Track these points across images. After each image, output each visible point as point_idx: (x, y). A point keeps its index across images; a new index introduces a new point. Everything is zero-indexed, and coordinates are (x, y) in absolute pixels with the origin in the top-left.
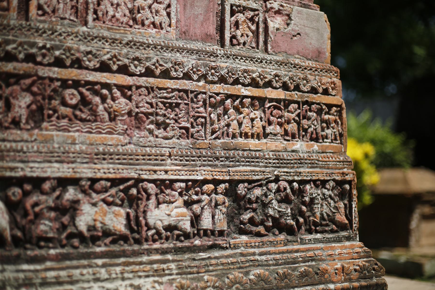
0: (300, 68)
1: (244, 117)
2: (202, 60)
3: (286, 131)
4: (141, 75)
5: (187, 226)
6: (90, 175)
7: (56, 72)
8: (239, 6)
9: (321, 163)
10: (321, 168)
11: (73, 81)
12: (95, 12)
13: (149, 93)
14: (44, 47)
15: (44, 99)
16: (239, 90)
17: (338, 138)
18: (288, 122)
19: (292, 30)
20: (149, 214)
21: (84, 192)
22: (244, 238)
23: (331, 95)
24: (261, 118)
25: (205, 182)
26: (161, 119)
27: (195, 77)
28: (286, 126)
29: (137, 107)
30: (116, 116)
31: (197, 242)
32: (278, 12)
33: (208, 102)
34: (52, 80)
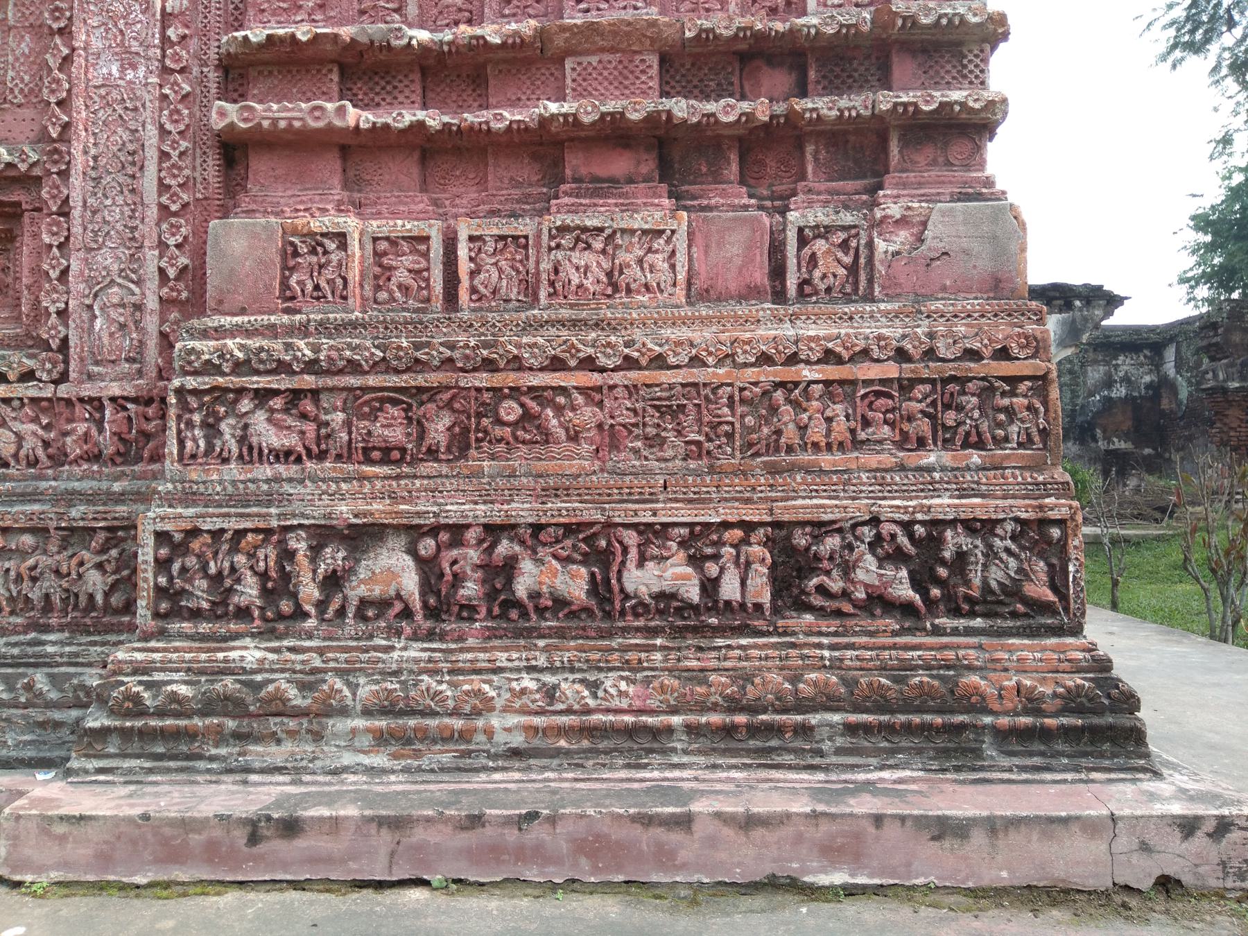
0: (942, 316)
1: (810, 418)
2: (728, 331)
3: (905, 436)
5: (693, 593)
6: (530, 520)
7: (482, 379)
8: (817, 226)
9: (984, 488)
10: (983, 496)
11: (511, 388)
12: (552, 284)
13: (630, 394)
14: (467, 346)
15: (469, 418)
16: (797, 372)
17: (1037, 439)
18: (910, 419)
19: (930, 249)
20: (625, 574)
21: (522, 543)
22: (809, 618)
23: (1018, 359)
24: (847, 417)
25: (726, 525)
26: (651, 431)
27: (710, 360)
28: (906, 426)
29: (612, 417)
30: (577, 433)
31: (713, 621)
32: (903, 222)
33: (737, 398)
34: (478, 390)
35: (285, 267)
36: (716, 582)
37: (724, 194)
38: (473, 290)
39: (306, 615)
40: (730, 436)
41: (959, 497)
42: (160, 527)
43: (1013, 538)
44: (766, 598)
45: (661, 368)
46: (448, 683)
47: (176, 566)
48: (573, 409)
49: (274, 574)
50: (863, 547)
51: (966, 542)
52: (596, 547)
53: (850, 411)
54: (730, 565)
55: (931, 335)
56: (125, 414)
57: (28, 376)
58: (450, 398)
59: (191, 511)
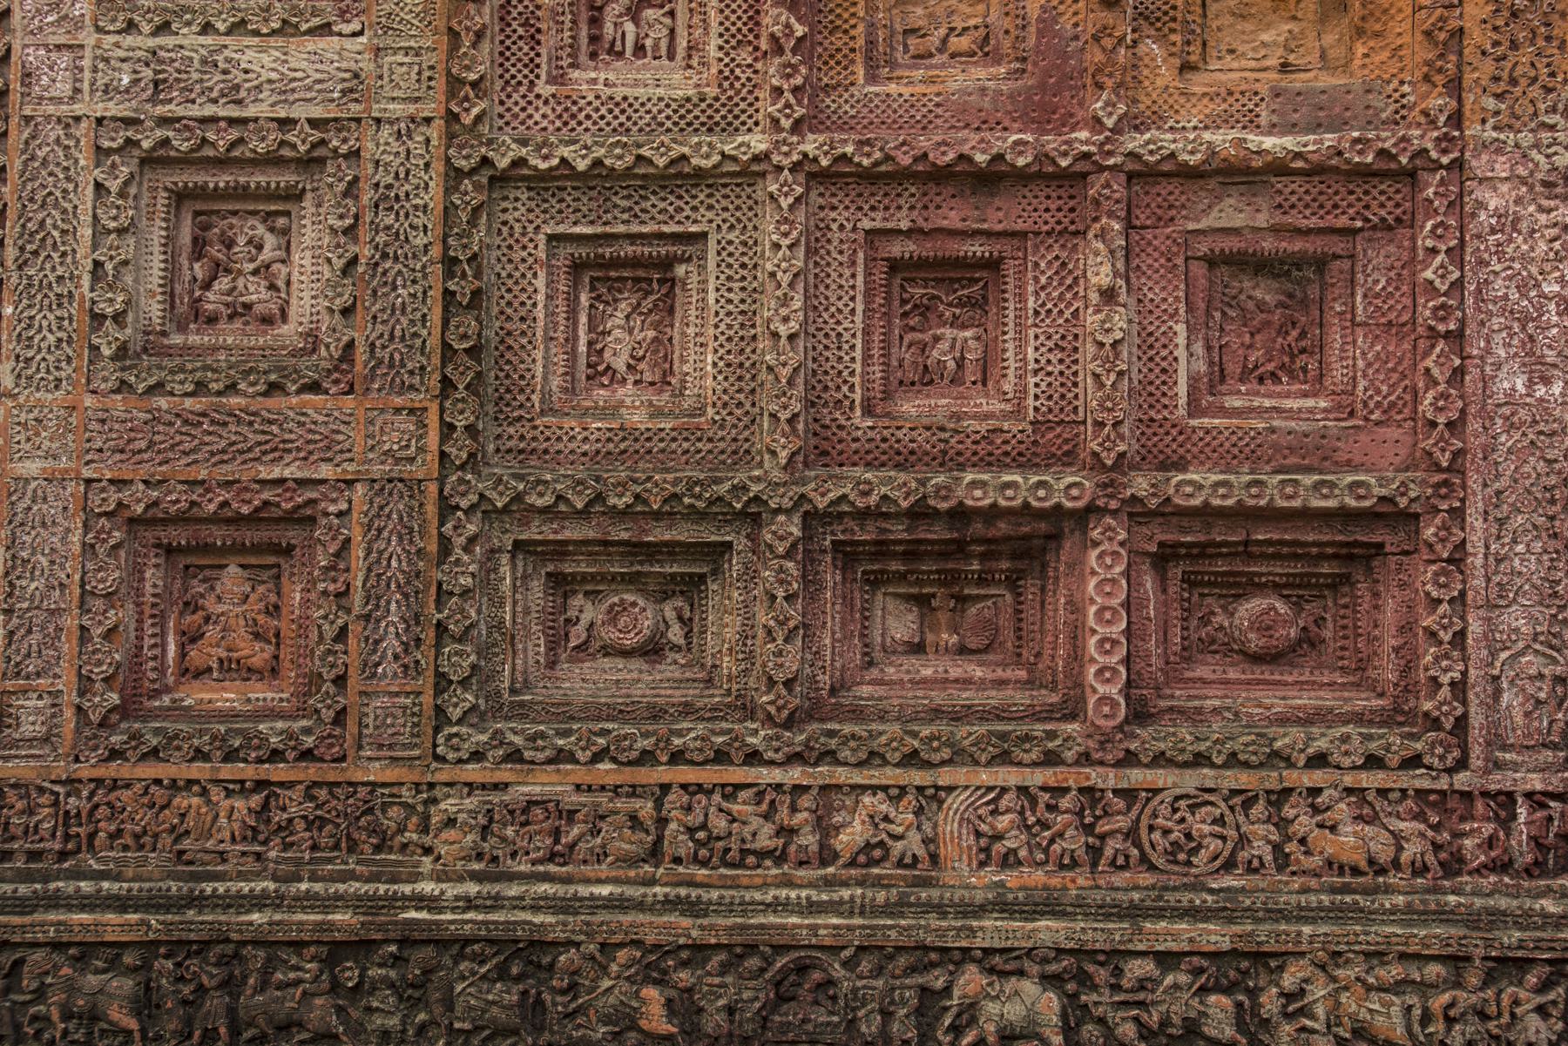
56: (1545, 813)
57: (1413, 762)
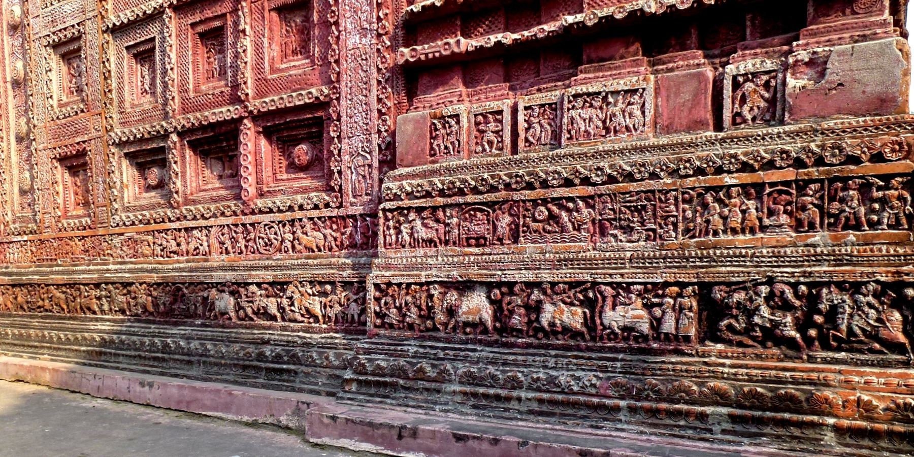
4: (603, 183)
5: (645, 328)
7: (527, 194)
9: (855, 259)
12: (569, 132)
20: (604, 314)
24: (757, 209)
25: (666, 284)
35: (431, 138)
36: (659, 321)
37: (684, 58)
38: (527, 140)
39: (438, 330)
40: (675, 225)
41: (835, 266)
42: (375, 281)
43: (874, 296)
44: (692, 332)
45: (632, 181)
46: (501, 371)
47: (383, 301)
48: (578, 211)
49: (424, 307)
50: (760, 300)
51: (837, 297)
52: (590, 298)
53: (759, 206)
54: (669, 311)
55: (823, 147)
58: (511, 206)
59: (388, 274)
